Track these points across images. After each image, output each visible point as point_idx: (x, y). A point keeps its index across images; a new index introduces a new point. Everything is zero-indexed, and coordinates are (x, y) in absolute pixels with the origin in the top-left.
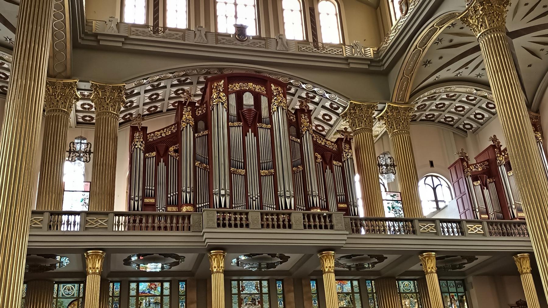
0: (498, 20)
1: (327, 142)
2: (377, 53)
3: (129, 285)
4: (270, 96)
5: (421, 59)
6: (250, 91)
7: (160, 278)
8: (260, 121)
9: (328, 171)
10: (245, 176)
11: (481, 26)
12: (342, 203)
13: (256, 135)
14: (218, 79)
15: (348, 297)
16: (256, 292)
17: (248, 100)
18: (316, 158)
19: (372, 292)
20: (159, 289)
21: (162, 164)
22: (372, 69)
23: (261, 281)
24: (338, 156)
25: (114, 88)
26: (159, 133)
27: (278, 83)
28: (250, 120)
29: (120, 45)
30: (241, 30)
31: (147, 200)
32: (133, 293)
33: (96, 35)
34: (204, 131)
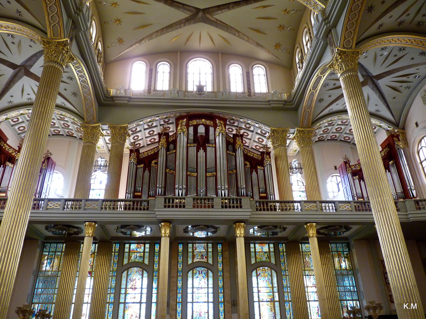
0: (351, 64)
1: (255, 155)
3: (125, 246)
4: (215, 126)
5: (316, 98)
7: (143, 242)
9: (254, 173)
10: (197, 177)
11: (340, 69)
12: (263, 193)
13: (205, 151)
15: (266, 255)
16: (204, 251)
17: (201, 130)
18: (245, 165)
19: (283, 252)
20: (143, 248)
21: (147, 172)
22: (286, 106)
23: (207, 243)
24: (261, 163)
26: (146, 153)
27: (220, 119)
29: (126, 102)
30: (200, 88)
31: (136, 194)
32: (127, 250)
33: (112, 97)
34: (172, 150)
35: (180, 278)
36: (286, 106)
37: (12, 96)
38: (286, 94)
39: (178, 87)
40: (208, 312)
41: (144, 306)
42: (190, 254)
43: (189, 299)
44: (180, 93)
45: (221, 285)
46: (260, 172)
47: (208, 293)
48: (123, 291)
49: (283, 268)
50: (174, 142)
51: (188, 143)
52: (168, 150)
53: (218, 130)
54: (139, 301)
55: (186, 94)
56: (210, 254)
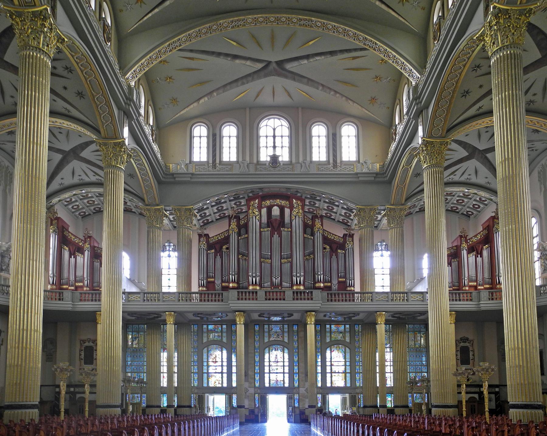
2: (382, 167)
4: (291, 208)
8: (283, 226)
9: (334, 257)
12: (342, 278)
13: (280, 236)
14: (254, 199)
17: (276, 211)
21: (218, 257)
22: (377, 179)
24: (342, 246)
25: (186, 209)
27: (297, 199)
28: (276, 225)
29: (189, 179)
33: (173, 174)
35: (257, 354)
36: (377, 179)
38: (378, 164)
39: (248, 159)
40: (284, 381)
41: (225, 375)
43: (267, 370)
44: (251, 166)
45: (296, 359)
46: (341, 257)
47: (284, 366)
48: (205, 364)
50: (246, 226)
52: (239, 234)
54: (220, 371)
55: (258, 167)
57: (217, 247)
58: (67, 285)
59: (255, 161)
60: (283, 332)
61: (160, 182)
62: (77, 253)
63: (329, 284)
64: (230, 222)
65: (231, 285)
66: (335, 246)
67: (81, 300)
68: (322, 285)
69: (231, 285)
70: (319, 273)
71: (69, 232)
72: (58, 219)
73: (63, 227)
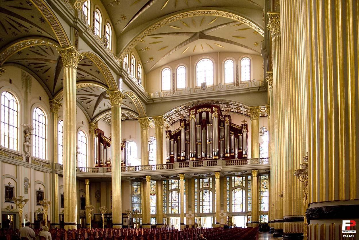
4: (212, 112)
6: (205, 111)
8: (208, 123)
13: (206, 129)
14: (192, 109)
15: (241, 182)
17: (204, 115)
19: (250, 180)
21: (176, 143)
24: (240, 131)
27: (215, 107)
29: (160, 101)
30: (204, 86)
33: (152, 99)
37: (100, 108)
40: (210, 210)
42: (201, 184)
46: (240, 137)
47: (210, 201)
49: (249, 188)
50: (189, 124)
51: (196, 125)
53: (213, 115)
56: (211, 184)
57: (174, 137)
58: (103, 163)
59: (195, 87)
60: (210, 182)
61: (146, 104)
62: (107, 147)
63: (233, 154)
64: (181, 123)
65: (181, 158)
66: (236, 131)
67: (107, 172)
68: (228, 155)
69: (181, 158)
70: (227, 148)
71: (103, 136)
72: (98, 129)
73: (101, 133)
